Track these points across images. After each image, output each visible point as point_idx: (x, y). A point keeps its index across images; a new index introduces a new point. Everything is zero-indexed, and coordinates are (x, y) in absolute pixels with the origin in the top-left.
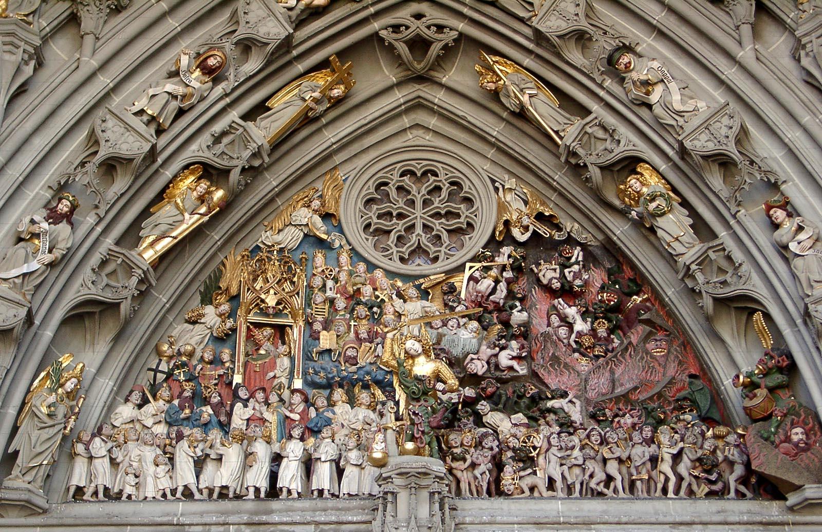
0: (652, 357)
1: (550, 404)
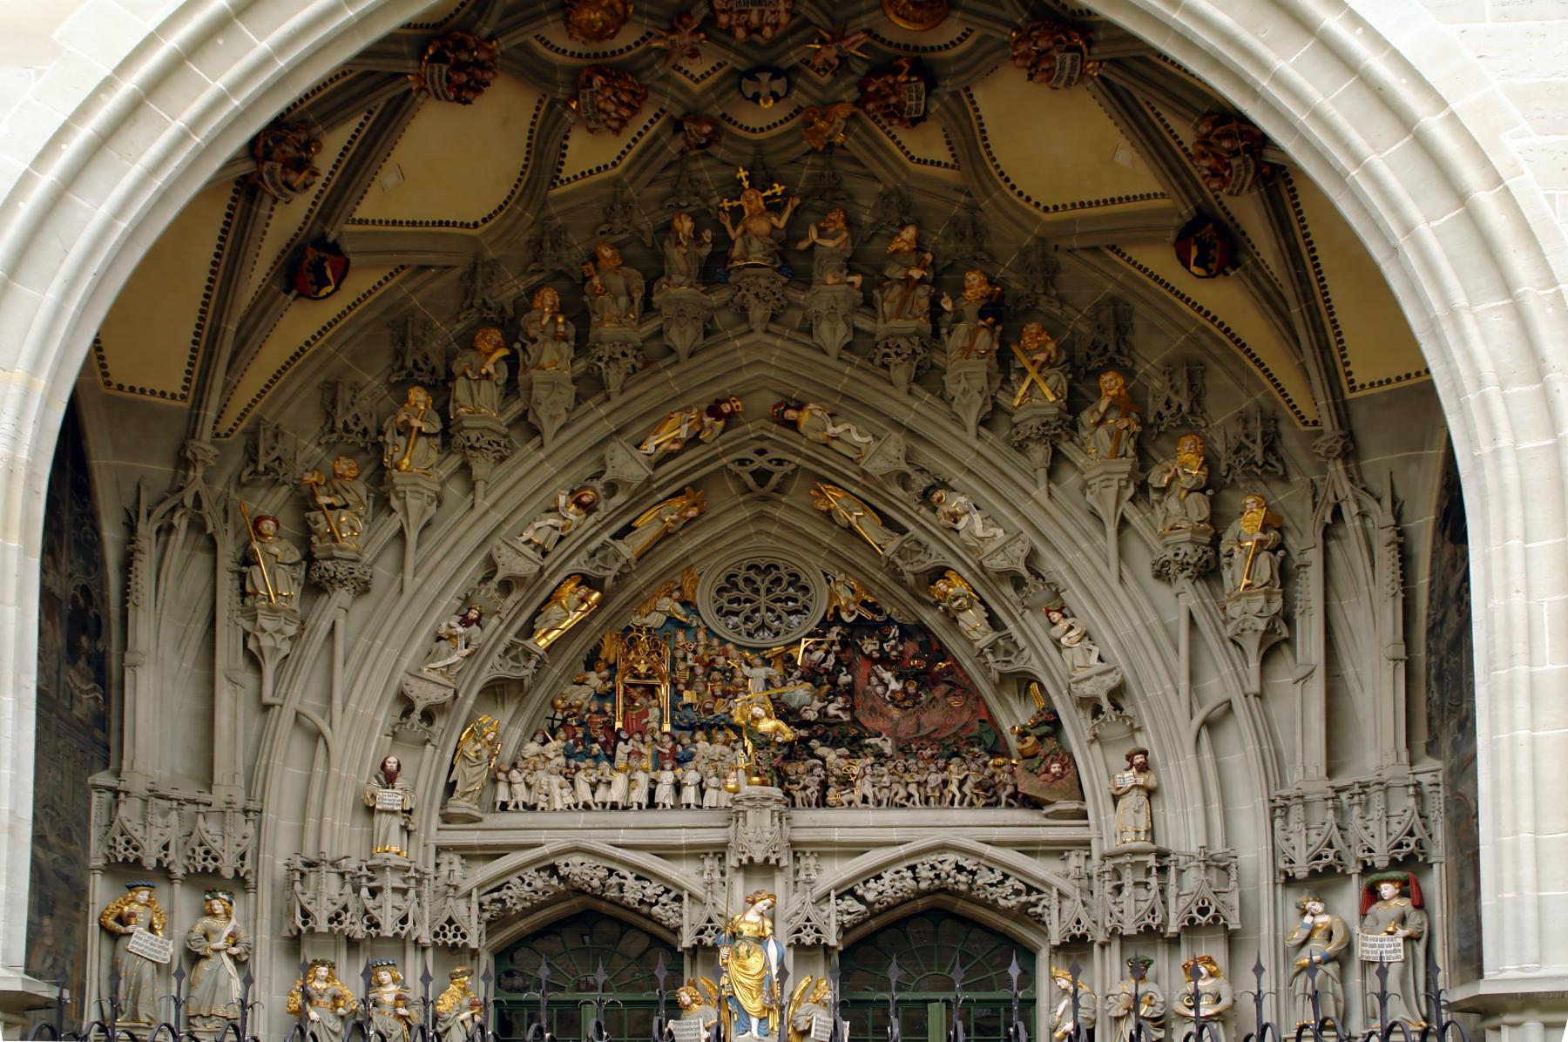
0: (951, 707)
1: (867, 741)
